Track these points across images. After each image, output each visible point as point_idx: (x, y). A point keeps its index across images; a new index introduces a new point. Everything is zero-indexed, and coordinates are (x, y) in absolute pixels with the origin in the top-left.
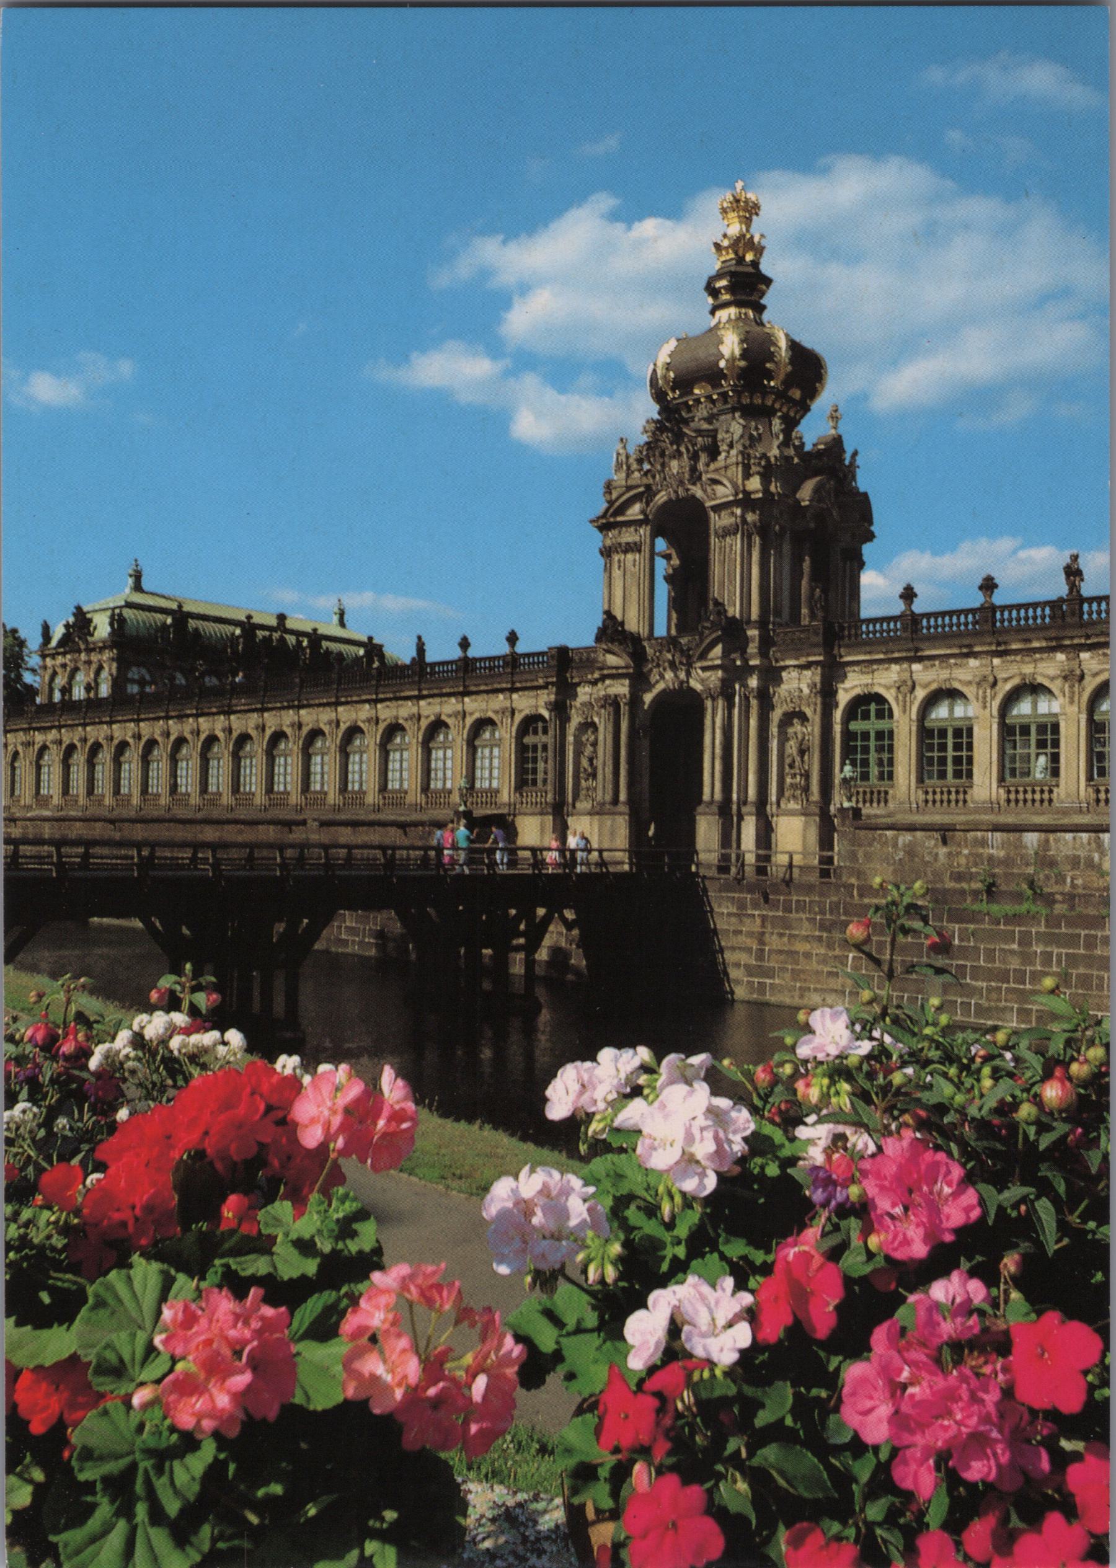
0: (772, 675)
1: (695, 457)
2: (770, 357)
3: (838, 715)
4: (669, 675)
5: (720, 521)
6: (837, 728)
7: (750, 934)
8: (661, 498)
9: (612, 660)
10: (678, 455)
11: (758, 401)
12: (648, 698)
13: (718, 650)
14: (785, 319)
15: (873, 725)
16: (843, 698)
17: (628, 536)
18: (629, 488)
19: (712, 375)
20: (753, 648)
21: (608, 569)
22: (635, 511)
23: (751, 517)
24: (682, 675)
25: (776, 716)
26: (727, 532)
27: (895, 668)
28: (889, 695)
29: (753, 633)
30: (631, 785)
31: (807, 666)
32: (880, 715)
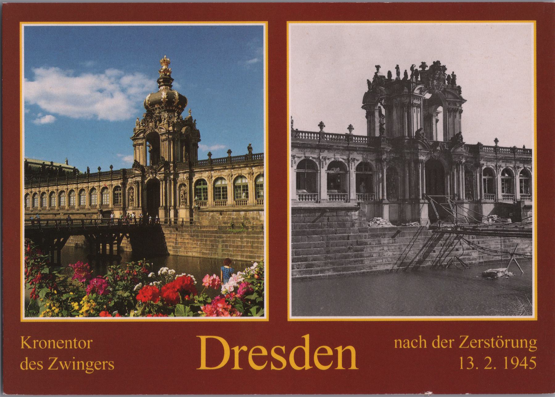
0: (176, 175)
1: (156, 123)
3: (193, 184)
4: (151, 175)
6: (193, 188)
7: (173, 238)
8: (148, 132)
9: (137, 172)
10: (152, 122)
11: (171, 108)
12: (146, 181)
13: (163, 169)
14: (177, 88)
15: (202, 187)
16: (194, 180)
17: (140, 142)
18: (140, 130)
19: (159, 102)
20: (171, 168)
21: (135, 149)
23: (170, 137)
24: (154, 176)
25: (178, 185)
26: (164, 140)
27: (207, 173)
28: (206, 179)
29: (171, 165)
31: (185, 173)
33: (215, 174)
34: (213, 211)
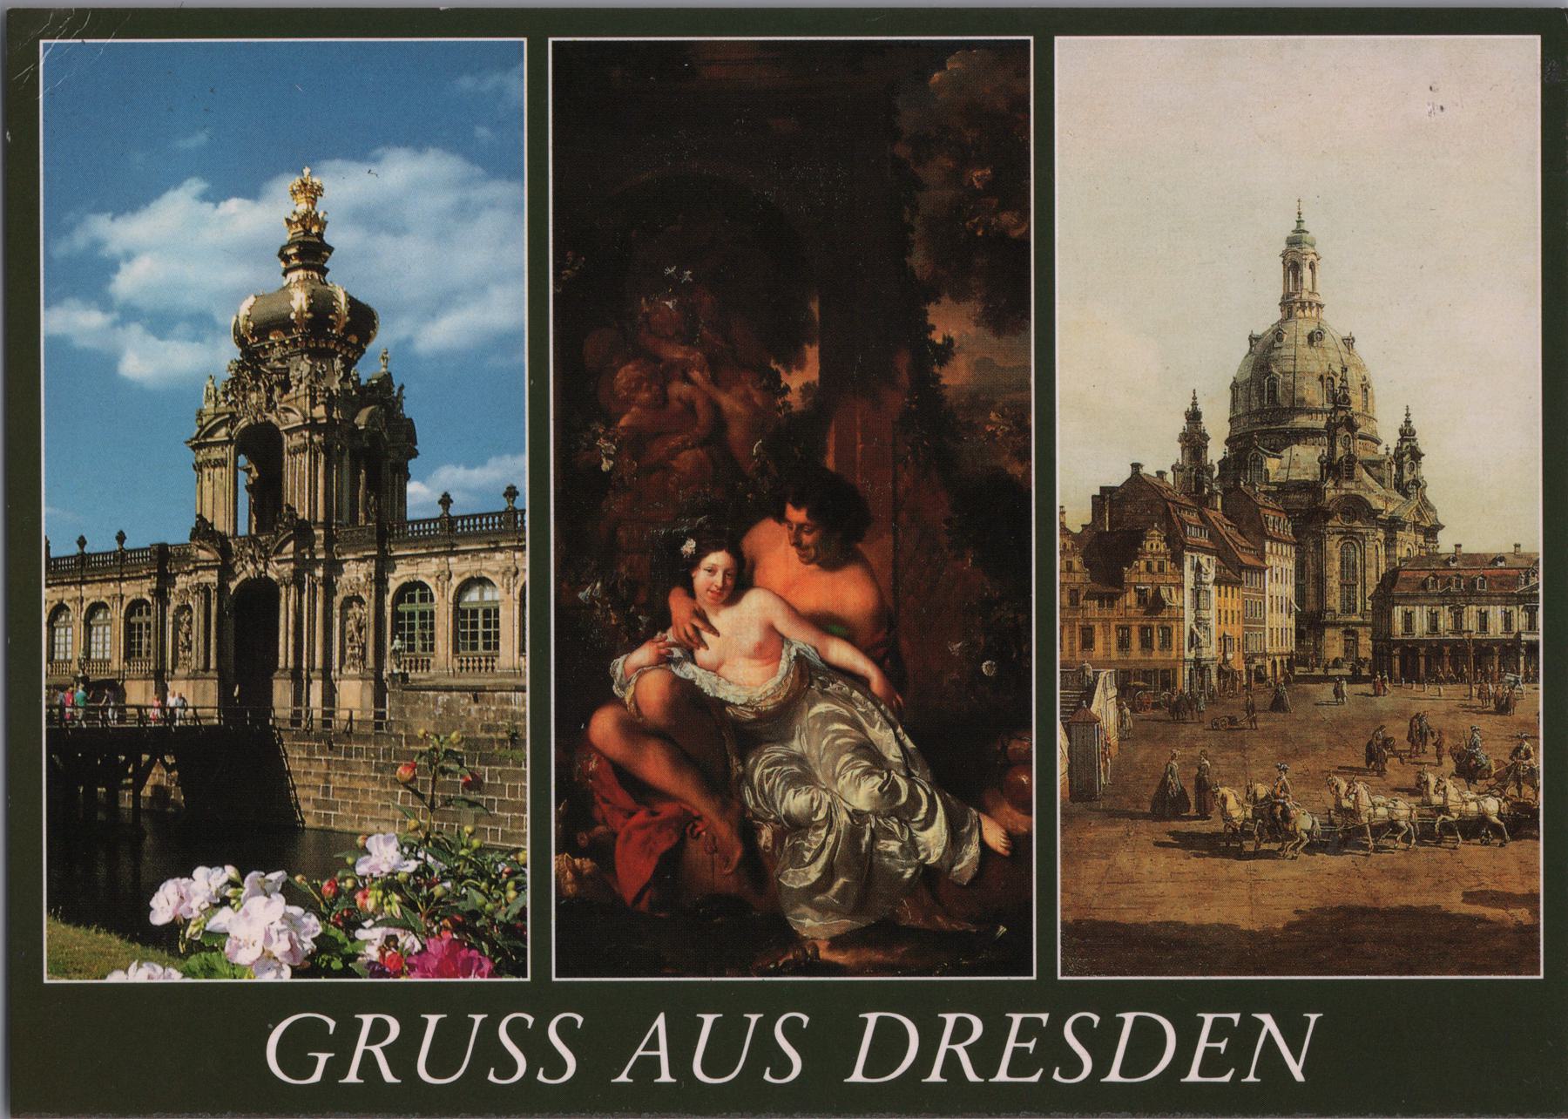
0: (334, 567)
1: (270, 390)
2: (332, 310)
3: (388, 599)
4: (250, 567)
5: (290, 442)
6: (388, 610)
8: (243, 423)
9: (203, 554)
12: (233, 585)
13: (290, 546)
15: (417, 607)
16: (393, 585)
17: (217, 454)
19: (283, 324)
20: (319, 545)
22: (221, 434)
23: (316, 438)
24: (261, 567)
25: (338, 600)
26: (295, 451)
27: (434, 560)
28: (431, 583)
29: (319, 532)
30: (219, 656)
31: (364, 559)
32: (423, 598)
33: (462, 567)
34: (449, 689)
